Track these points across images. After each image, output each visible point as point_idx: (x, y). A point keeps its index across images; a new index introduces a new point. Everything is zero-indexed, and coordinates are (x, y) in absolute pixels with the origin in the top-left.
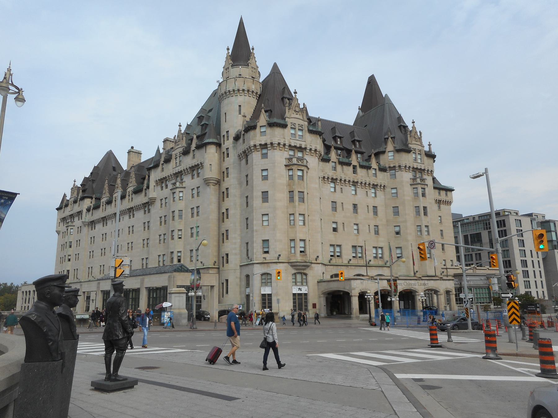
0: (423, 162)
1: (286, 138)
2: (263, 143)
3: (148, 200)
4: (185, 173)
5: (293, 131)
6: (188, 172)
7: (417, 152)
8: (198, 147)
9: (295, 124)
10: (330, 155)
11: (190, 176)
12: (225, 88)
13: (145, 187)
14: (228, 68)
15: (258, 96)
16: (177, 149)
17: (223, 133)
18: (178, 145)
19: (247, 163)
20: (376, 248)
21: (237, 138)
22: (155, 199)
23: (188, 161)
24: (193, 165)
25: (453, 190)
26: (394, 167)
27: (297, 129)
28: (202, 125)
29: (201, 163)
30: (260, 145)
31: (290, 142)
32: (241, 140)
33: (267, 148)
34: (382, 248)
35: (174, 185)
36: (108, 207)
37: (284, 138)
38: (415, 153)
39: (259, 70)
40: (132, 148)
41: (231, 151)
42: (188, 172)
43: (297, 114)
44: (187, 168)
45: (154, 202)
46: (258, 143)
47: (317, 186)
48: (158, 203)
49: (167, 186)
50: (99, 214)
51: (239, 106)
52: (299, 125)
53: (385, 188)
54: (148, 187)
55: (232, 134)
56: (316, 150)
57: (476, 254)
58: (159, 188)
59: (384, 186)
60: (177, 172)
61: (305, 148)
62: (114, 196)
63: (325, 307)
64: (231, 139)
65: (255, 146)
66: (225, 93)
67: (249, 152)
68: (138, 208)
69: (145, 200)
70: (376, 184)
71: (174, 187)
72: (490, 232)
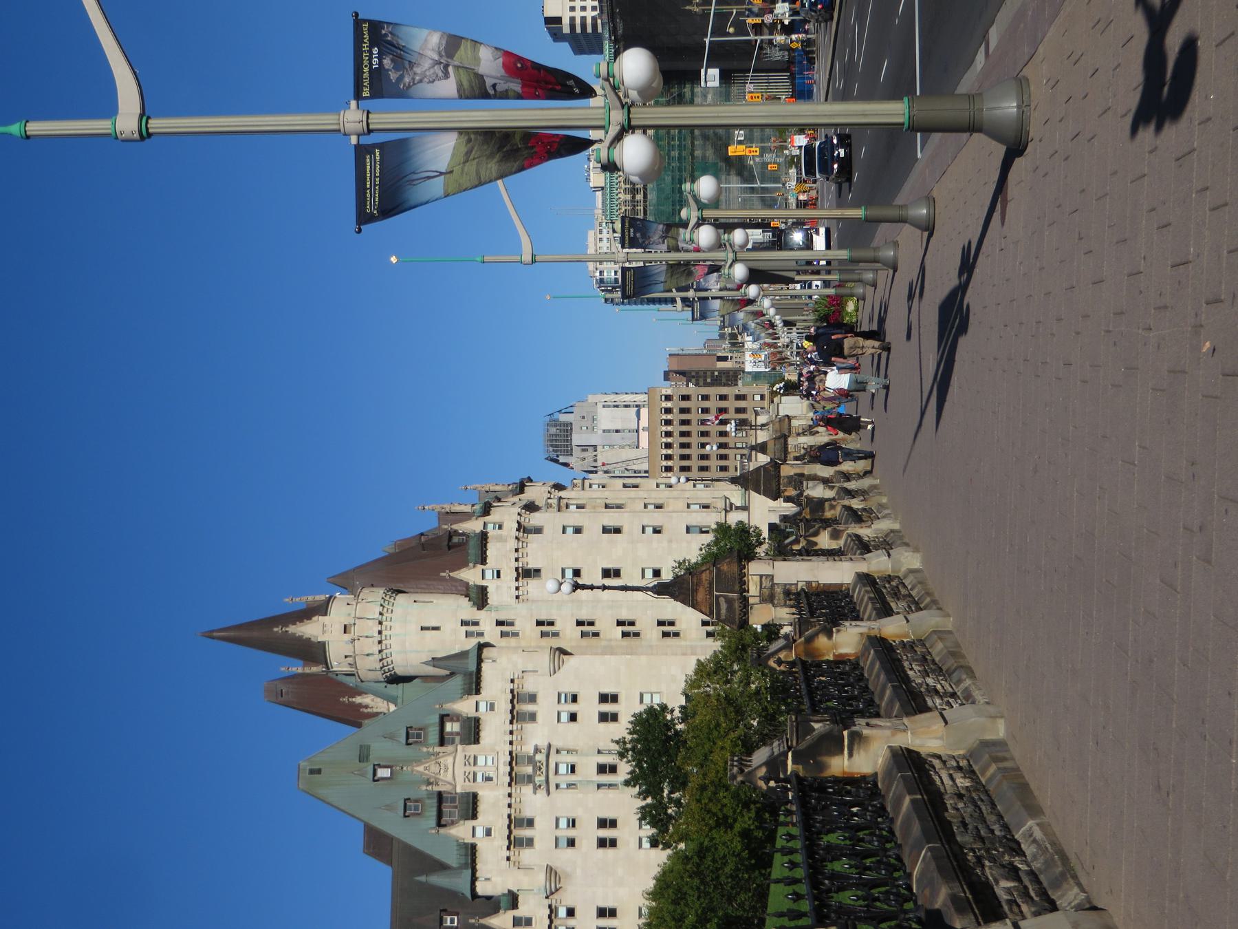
2: (516, 525)
12: (370, 623)
14: (324, 626)
18: (447, 769)
21: (480, 598)
22: (551, 869)
24: (510, 706)
30: (518, 530)
41: (502, 617)
45: (556, 873)
46: (515, 533)
54: (513, 900)
60: (508, 769)
64: (481, 615)
66: (380, 623)
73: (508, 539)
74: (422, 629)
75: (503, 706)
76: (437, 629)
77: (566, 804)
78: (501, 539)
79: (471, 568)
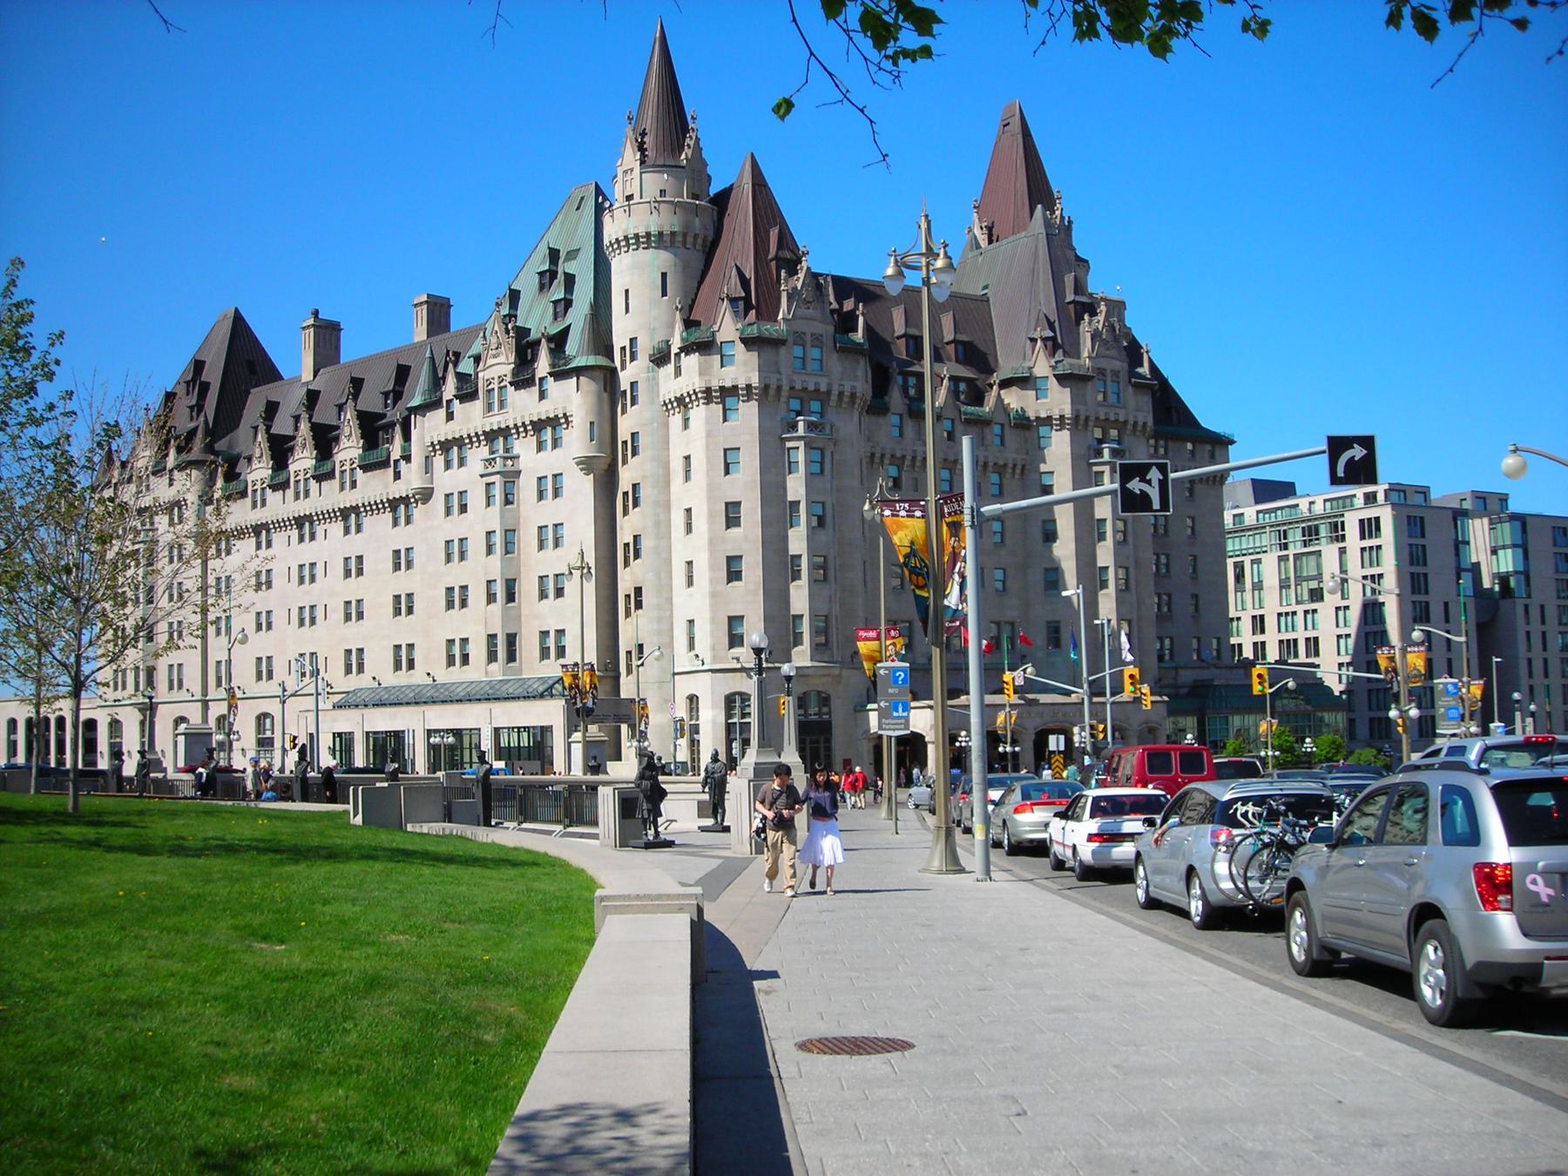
0: (1122, 401)
1: (783, 370)
2: (728, 384)
3: (407, 490)
4: (518, 433)
5: (798, 351)
6: (526, 431)
7: (1109, 378)
8: (559, 375)
9: (804, 333)
10: (886, 398)
11: (532, 441)
13: (396, 453)
14: (632, 170)
15: (708, 244)
16: (493, 368)
17: (619, 340)
19: (686, 421)
20: (998, 624)
23: (523, 405)
25: (1232, 442)
26: (1050, 418)
27: (808, 346)
28: (555, 303)
29: (565, 414)
30: (722, 388)
31: (792, 381)
32: (670, 368)
33: (738, 395)
34: (1012, 624)
35: (490, 464)
36: (273, 498)
37: (779, 372)
38: (1105, 381)
39: (710, 170)
40: (316, 314)
42: (526, 431)
43: (808, 308)
44: (523, 423)
46: (715, 384)
47: (855, 483)
48: (438, 501)
49: (462, 462)
50: (240, 514)
51: (662, 274)
52: (812, 335)
53: (1026, 472)
55: (645, 349)
56: (853, 396)
57: (1306, 612)
58: (439, 461)
59: (1023, 467)
61: (829, 392)
62: (292, 468)
63: (872, 767)
65: (708, 391)
67: (691, 401)
68: (374, 508)
69: (399, 490)
70: (1001, 463)
71: (490, 470)
72: (1342, 551)
73: (707, 378)
74: (627, 291)
75: (545, 410)
76: (627, 311)
77: (476, 499)
78: (703, 372)
79: (681, 335)
